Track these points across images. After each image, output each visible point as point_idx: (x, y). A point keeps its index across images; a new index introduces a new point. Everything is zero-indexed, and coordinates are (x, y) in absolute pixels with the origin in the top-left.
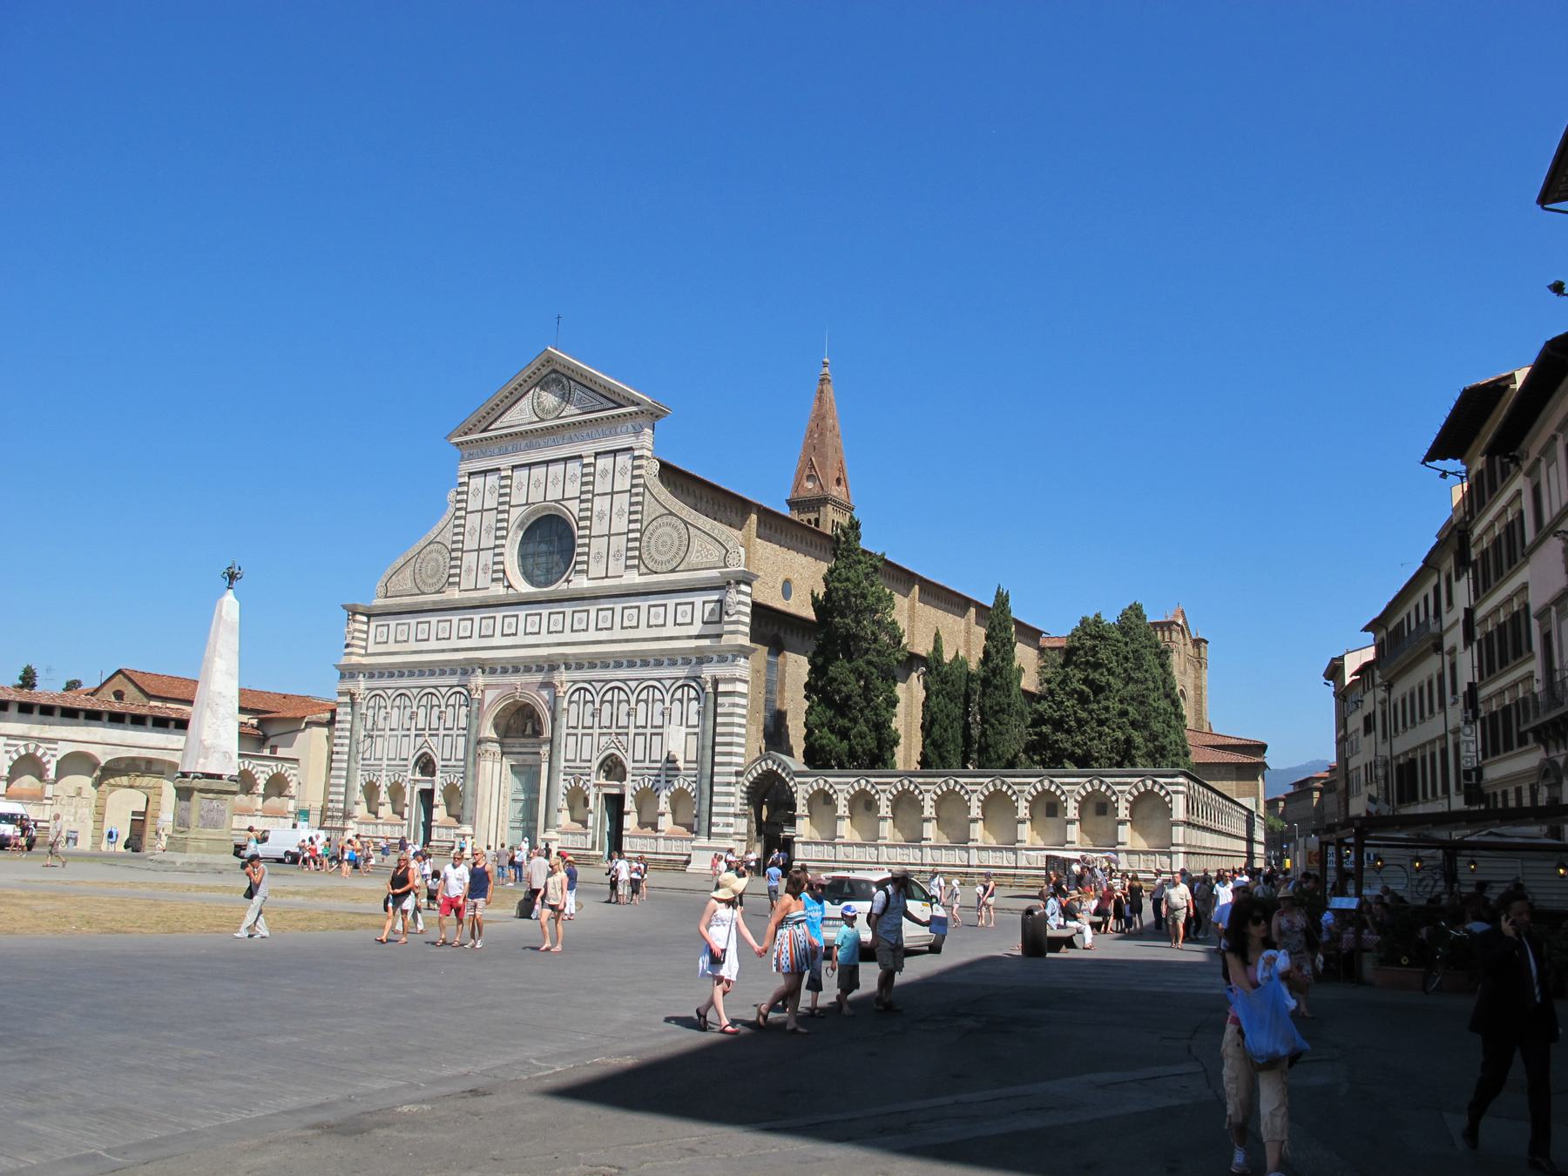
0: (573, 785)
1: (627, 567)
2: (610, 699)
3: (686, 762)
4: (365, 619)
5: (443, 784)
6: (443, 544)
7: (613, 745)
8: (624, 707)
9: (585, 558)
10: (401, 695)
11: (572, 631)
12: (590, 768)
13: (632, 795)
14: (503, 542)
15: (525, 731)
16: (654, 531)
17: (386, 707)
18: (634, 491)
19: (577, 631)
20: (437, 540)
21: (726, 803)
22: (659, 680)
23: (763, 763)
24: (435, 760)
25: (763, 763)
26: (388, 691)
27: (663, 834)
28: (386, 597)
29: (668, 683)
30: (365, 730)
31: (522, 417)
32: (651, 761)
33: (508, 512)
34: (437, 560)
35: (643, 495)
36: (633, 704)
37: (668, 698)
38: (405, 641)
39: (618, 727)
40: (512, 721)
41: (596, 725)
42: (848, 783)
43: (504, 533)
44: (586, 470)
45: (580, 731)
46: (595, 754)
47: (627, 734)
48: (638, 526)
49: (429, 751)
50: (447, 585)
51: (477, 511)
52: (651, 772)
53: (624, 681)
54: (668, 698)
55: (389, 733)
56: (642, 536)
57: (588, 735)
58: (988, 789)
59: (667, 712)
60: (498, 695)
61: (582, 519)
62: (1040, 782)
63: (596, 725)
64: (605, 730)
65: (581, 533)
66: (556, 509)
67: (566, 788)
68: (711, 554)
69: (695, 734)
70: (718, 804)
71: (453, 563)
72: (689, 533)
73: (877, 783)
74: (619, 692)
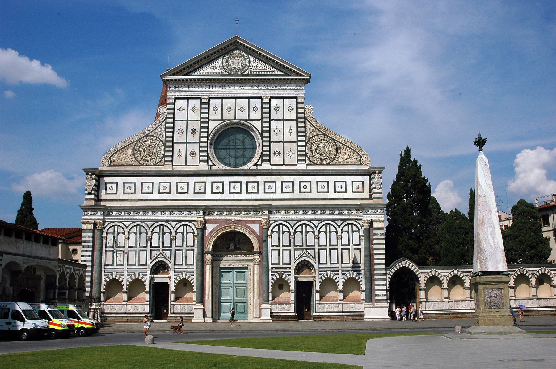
0: (278, 277)
1: (298, 160)
2: (301, 230)
3: (353, 263)
4: (97, 178)
5: (176, 279)
6: (157, 137)
7: (305, 255)
8: (310, 235)
9: (268, 153)
10: (136, 226)
11: (265, 192)
12: (290, 268)
13: (319, 282)
14: (206, 139)
15: (229, 247)
16: (314, 142)
17: (124, 233)
18: (299, 120)
19: (268, 193)
20: (152, 134)
21: (383, 284)
22: (333, 221)
23: (400, 264)
24: (170, 265)
25: (400, 264)
26: (127, 224)
27: (342, 302)
28: (110, 166)
29: (339, 223)
30: (106, 246)
31: (216, 71)
32: (331, 264)
33: (208, 123)
34: (153, 147)
35: (305, 122)
36: (317, 233)
37: (339, 231)
38: (132, 193)
39: (307, 245)
40: (218, 242)
41: (292, 244)
42: (449, 272)
43: (206, 134)
44: (264, 106)
45: (281, 248)
46: (292, 262)
47: (314, 249)
48: (303, 139)
49: (164, 260)
50: (163, 161)
51: (182, 120)
52: (332, 269)
53: (310, 221)
54: (339, 231)
55: (126, 249)
56: (306, 144)
57: (287, 250)
58: (517, 273)
59: (339, 238)
60: (217, 227)
61: (263, 132)
62: (541, 269)
63: (292, 244)
64: (298, 247)
65: (264, 139)
66: (243, 124)
67: (273, 279)
68: (352, 158)
69: (358, 249)
70: (378, 285)
71: (167, 149)
72: (336, 145)
73: (463, 272)
74: (306, 227)
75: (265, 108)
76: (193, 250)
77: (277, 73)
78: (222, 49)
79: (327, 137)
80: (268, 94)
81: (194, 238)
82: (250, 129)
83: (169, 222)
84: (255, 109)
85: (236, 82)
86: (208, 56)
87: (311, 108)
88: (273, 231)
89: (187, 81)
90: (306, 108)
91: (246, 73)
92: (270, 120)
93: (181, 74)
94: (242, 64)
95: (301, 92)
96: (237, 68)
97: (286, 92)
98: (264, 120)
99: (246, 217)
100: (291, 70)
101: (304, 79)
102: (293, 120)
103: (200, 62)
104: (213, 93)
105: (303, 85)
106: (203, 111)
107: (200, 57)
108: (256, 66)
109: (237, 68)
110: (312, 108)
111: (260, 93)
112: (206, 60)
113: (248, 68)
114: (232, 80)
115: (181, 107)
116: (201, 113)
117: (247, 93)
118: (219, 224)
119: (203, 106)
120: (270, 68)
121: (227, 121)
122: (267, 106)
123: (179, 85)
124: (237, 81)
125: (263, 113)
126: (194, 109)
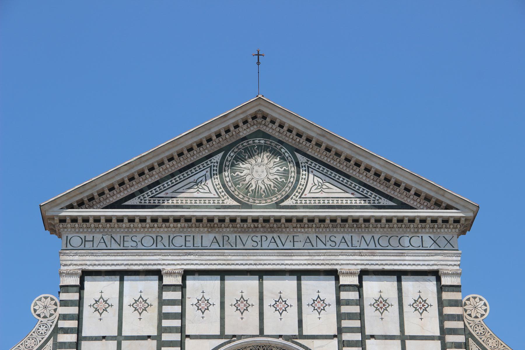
44: (345, 295)
51: (104, 337)
75: (348, 303)
77: (376, 202)
78: (218, 135)
80: (356, 262)
84: (319, 305)
85: (262, 227)
86: (180, 154)
87: (482, 303)
89: (120, 224)
90: (468, 302)
91: (288, 202)
92: (365, 337)
93: (100, 202)
94: (278, 177)
95: (450, 258)
96: (263, 187)
97: (407, 258)
98: (346, 337)
100: (417, 194)
101: (457, 221)
102: (431, 338)
103: (157, 169)
104: (197, 257)
105: (456, 237)
106: (166, 309)
107: (158, 155)
108: (316, 183)
109: (263, 187)
110: (485, 305)
111: (332, 260)
113: (294, 188)
114: (249, 220)
115: (101, 297)
116: (162, 316)
117: (294, 258)
119: (167, 295)
120: (357, 187)
121: (238, 340)
122: (353, 295)
123: (95, 235)
124: (264, 224)
125: (340, 317)
126: (140, 305)
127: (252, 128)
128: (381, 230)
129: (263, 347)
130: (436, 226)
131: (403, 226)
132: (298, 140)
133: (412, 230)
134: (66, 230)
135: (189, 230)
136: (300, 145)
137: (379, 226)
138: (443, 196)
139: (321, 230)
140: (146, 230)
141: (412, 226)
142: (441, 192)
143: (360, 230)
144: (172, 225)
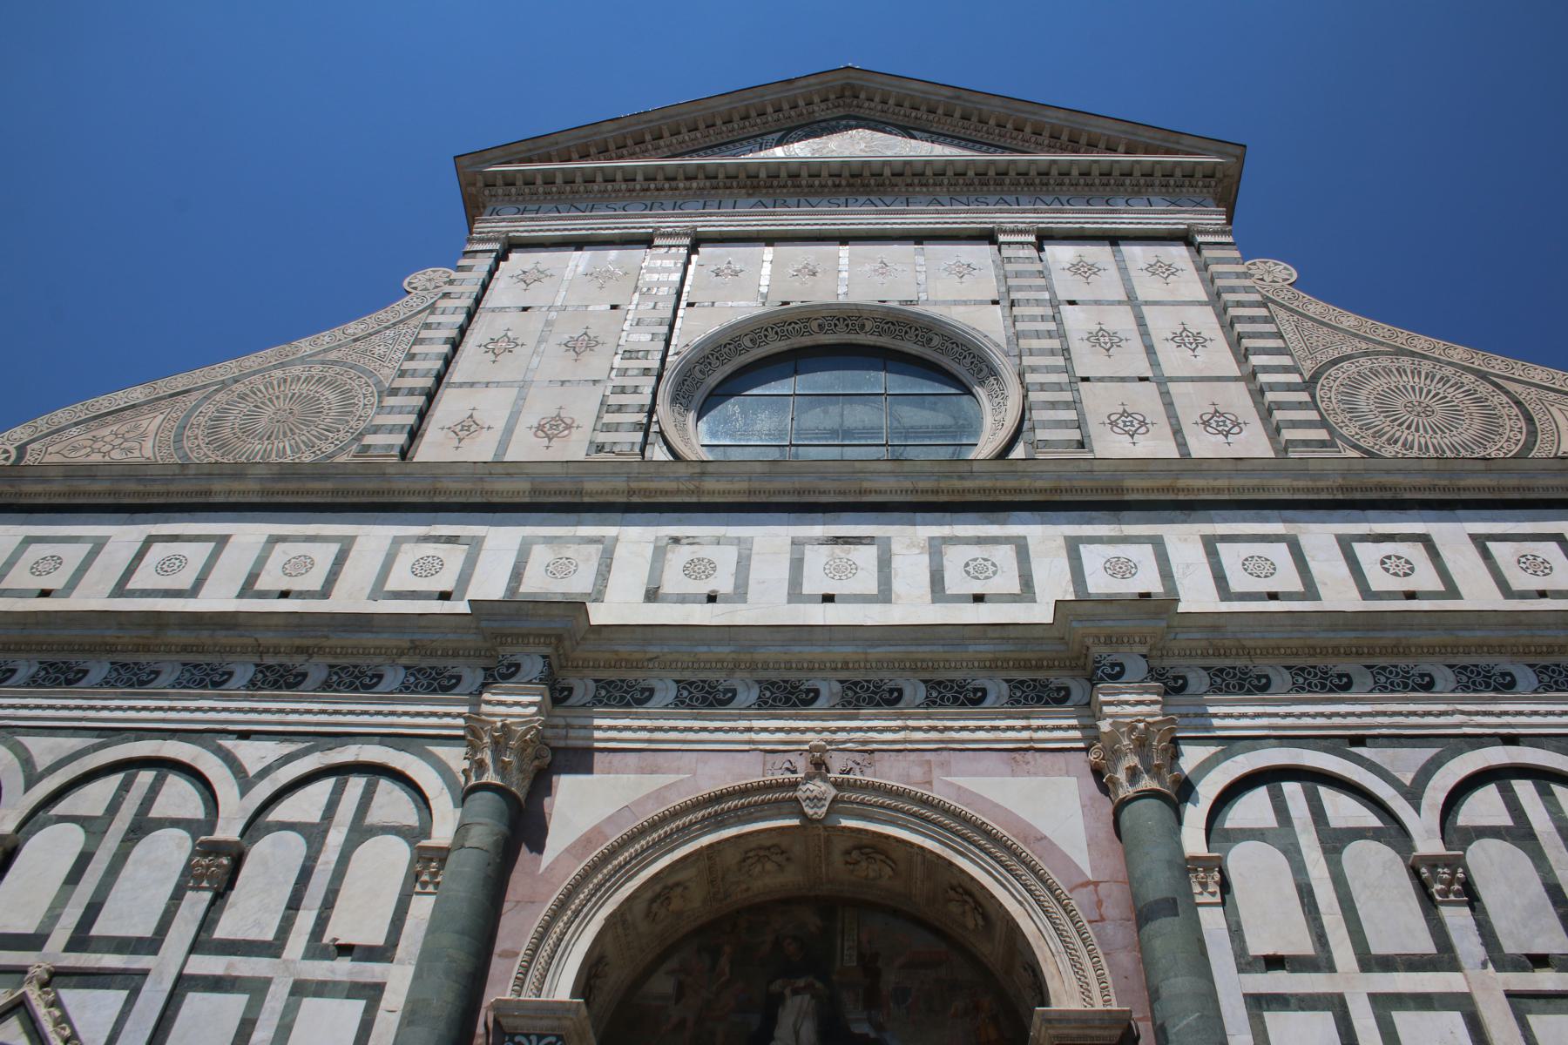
40: (662, 984)
57: (1425, 1002)
60: (658, 795)
72: (1507, 393)
74: (1546, 795)
76: (372, 993)
79: (1427, 362)
81: (413, 877)
82: (936, 341)
83: (229, 744)
85: (850, 185)
88: (1228, 825)
99: (939, 724)
112: (699, 135)
118: (672, 778)
124: (851, 181)
127: (835, 110)
128: (1072, 188)
129: (845, 320)
130: (1172, 182)
131: (1112, 182)
132: (913, 115)
133: (1129, 190)
134: (494, 199)
135: (713, 192)
136: (918, 122)
137: (1067, 180)
138: (1178, 143)
139: (958, 189)
140: (634, 194)
141: (1128, 182)
142: (1174, 137)
143: (1032, 188)
144: (681, 185)
